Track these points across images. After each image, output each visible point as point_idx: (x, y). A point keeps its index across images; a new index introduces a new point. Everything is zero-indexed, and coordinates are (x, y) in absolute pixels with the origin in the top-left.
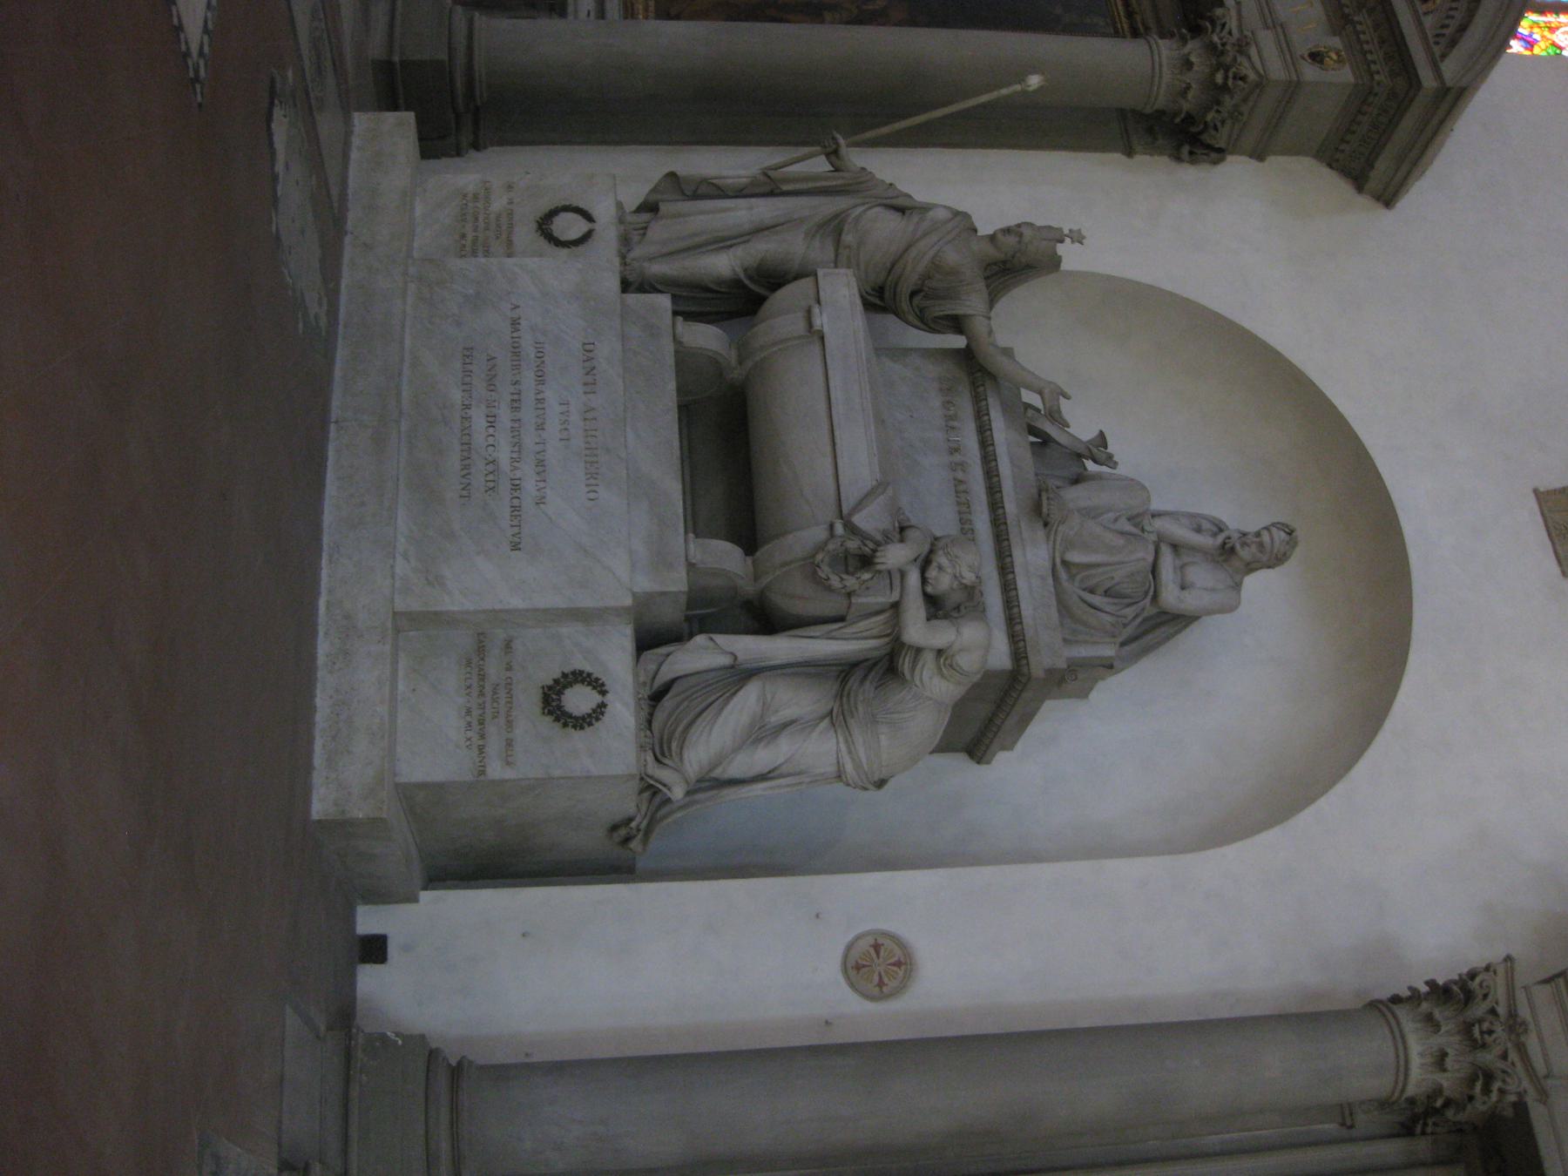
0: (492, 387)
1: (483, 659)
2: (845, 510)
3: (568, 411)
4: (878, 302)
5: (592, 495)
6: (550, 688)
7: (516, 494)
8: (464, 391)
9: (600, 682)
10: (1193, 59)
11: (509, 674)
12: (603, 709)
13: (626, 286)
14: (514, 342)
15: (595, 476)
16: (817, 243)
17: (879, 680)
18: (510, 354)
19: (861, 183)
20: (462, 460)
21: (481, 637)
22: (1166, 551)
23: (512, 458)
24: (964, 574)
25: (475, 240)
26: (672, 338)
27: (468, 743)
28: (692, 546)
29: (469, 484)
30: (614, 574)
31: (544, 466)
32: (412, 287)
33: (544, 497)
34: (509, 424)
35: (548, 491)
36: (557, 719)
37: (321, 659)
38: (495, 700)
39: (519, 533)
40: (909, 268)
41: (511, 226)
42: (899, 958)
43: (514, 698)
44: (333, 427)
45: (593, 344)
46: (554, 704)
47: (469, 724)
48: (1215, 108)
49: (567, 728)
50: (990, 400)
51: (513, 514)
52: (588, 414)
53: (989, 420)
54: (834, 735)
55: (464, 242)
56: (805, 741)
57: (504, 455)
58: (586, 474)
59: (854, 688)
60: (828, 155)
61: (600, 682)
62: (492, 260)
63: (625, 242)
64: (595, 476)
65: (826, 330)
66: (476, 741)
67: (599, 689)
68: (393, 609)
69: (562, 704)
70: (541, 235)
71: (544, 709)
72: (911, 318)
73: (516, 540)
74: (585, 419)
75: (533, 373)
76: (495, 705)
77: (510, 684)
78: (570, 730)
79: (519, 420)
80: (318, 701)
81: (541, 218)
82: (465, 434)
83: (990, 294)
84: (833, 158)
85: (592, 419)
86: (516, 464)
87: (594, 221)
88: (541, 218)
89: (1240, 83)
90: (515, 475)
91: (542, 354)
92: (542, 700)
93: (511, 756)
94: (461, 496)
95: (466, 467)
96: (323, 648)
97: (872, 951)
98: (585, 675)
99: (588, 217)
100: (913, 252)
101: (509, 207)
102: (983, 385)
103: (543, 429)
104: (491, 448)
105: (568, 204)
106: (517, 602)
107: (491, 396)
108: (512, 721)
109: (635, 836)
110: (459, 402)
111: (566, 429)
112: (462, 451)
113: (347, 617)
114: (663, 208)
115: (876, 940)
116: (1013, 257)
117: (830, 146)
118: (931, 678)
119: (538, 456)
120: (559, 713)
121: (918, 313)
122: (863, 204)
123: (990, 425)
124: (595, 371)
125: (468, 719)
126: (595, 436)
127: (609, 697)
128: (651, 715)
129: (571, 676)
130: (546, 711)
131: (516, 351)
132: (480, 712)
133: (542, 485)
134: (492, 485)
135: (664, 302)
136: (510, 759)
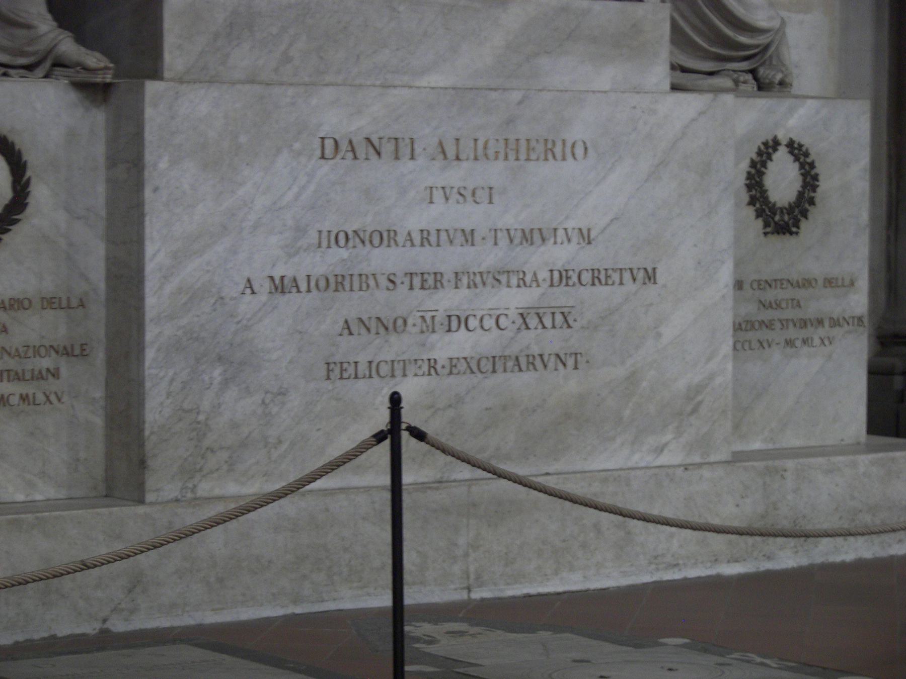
0: (400, 322)
3: (443, 188)
5: (579, 151)
6: (766, 225)
7: (575, 278)
8: (405, 375)
12: (796, 146)
14: (317, 286)
18: (342, 295)
20: (520, 370)
23: (519, 286)
27: (827, 342)
29: (558, 356)
30: (693, 120)
31: (532, 230)
33: (580, 230)
34: (464, 292)
35: (570, 224)
36: (805, 214)
38: (779, 306)
43: (779, 277)
44: (478, 594)
47: (805, 341)
49: (817, 200)
51: (603, 281)
55: (15, 400)
58: (546, 159)
61: (762, 147)
62: (149, 336)
66: (822, 332)
67: (770, 150)
68: (726, 462)
69: (787, 205)
71: (791, 233)
73: (641, 275)
74: (458, 158)
76: (784, 305)
77: (759, 281)
78: (818, 195)
79: (456, 273)
82: (479, 369)
86: (528, 279)
90: (544, 280)
91: (342, 237)
93: (843, 279)
94: (576, 368)
95: (531, 364)
104: (503, 321)
106: (726, 274)
107: (414, 325)
110: (424, 380)
111: (474, 194)
112: (505, 371)
119: (517, 241)
120: (797, 212)
125: (798, 343)
129: (754, 192)
130: (794, 229)
132: (791, 325)
133: (561, 233)
136: (847, 282)
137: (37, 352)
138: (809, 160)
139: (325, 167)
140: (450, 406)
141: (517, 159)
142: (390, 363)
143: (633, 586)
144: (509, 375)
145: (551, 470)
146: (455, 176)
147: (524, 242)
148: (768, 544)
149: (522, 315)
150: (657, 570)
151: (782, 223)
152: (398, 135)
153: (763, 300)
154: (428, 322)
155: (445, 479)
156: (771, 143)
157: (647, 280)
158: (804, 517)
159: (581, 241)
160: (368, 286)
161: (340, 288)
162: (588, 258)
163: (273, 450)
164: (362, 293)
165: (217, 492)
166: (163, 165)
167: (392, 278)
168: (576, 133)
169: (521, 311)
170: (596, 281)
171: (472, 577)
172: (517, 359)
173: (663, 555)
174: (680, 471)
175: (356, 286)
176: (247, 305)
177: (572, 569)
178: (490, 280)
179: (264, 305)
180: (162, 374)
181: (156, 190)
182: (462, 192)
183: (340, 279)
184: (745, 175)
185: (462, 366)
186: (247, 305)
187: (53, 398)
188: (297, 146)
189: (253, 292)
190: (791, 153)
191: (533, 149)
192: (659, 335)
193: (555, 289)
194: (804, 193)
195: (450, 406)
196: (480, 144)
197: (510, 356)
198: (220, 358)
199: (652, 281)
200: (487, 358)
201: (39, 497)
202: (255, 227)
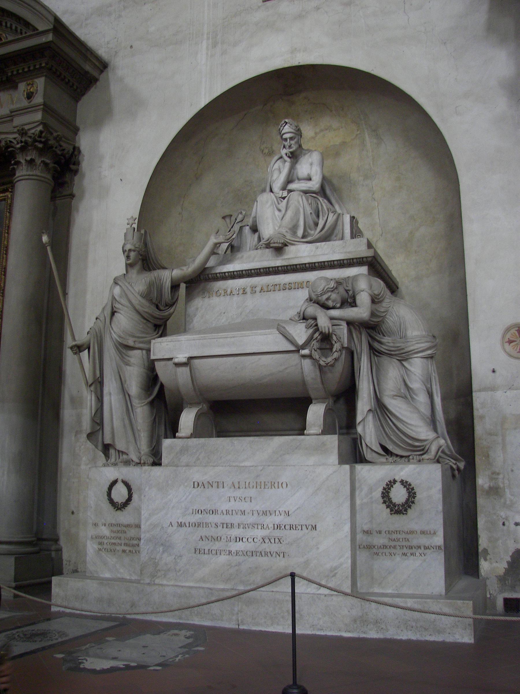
0: (219, 538)
1: (374, 547)
2: (293, 348)
3: (234, 497)
4: (162, 328)
5: (284, 485)
6: (391, 510)
7: (283, 527)
8: (220, 554)
9: (388, 483)
10: (29, 158)
11: (383, 532)
12: (404, 482)
13: (157, 463)
15: (273, 484)
16: (132, 360)
17: (380, 334)
18: (200, 528)
19: (97, 334)
20: (262, 556)
21: (362, 547)
22: (291, 186)
23: (261, 529)
24: (332, 287)
25: (126, 545)
26: (189, 439)
27: (423, 555)
28: (312, 432)
31: (266, 511)
32: (157, 581)
33: (285, 511)
34: (241, 530)
36: (410, 507)
37: (380, 636)
39: (306, 526)
40: (146, 310)
41: (119, 525)
42: (516, 330)
43: (398, 529)
44: (241, 627)
45: (194, 482)
46: (401, 508)
48: (54, 149)
50: (218, 271)
51: (294, 528)
52: (236, 486)
53: (228, 272)
54: (413, 359)
55: (127, 551)
56: (415, 375)
57: (259, 533)
59: (386, 348)
60: (80, 351)
61: (388, 483)
62: (142, 537)
63: (128, 463)
64: (273, 484)
65: (187, 355)
67: (392, 484)
69: (401, 504)
70: (125, 509)
71: (403, 514)
72: (172, 310)
73: (310, 527)
75: (211, 516)
76: (401, 540)
80: (404, 638)
81: (114, 508)
83: (159, 269)
84: (82, 349)
85: (239, 484)
86: (265, 527)
87: (117, 479)
88: (114, 508)
89: (43, 135)
90: (271, 527)
92: (399, 514)
95: (266, 554)
96: (373, 634)
97: (512, 344)
98: (384, 491)
99: (115, 482)
100: (138, 307)
101: (107, 525)
102: (208, 275)
103: (244, 511)
105: (106, 494)
107: (224, 539)
108: (410, 531)
109: (457, 466)
110: (227, 557)
111: (245, 499)
113: (355, 621)
114: (107, 441)
115: (506, 342)
116: (141, 255)
117: (76, 350)
118: (383, 307)
119: (261, 514)
120: (406, 506)
121: (168, 307)
122: (111, 333)
123: (231, 272)
124: (211, 482)
126: (249, 483)
127: (397, 478)
128: (397, 456)
129: (385, 499)
130: (405, 512)
131: (198, 525)
132: (405, 548)
133: (277, 512)
134: (277, 540)
135: (167, 443)
136: (432, 532)
137: (133, 539)
138: (411, 487)
139: (195, 490)
140: (236, 565)
141: (261, 488)
142: (216, 551)
143: (303, 634)
144: (257, 557)
145: (274, 590)
146: (238, 493)
147: (263, 514)
148: (364, 628)
149: (263, 538)
150: (314, 630)
151: (399, 510)
152: (219, 481)
153: (391, 538)
154: (229, 538)
155: (235, 588)
156: (392, 481)
157: (312, 529)
158: (381, 619)
159: (285, 515)
160: (208, 527)
161: (199, 526)
162: (288, 521)
163: (178, 573)
164: (206, 528)
165: (161, 582)
166: (147, 489)
167: (216, 524)
168: (283, 479)
169: (263, 537)
170: (292, 528)
171: (240, 621)
172: (261, 552)
173: (316, 625)
174: (323, 597)
175: (204, 526)
176: (170, 530)
177: (278, 624)
178: (251, 526)
179: (176, 530)
180: (145, 547)
181: (145, 496)
182: (240, 498)
183: (199, 524)
184: (381, 493)
185: (241, 553)
186: (170, 530)
187: (137, 552)
188: (186, 484)
189: (172, 526)
190: (402, 484)
191: (267, 485)
192: (318, 548)
193: (275, 530)
194: (409, 499)
195: (236, 565)
196: (247, 484)
197: (258, 552)
198: (162, 544)
199: (315, 529)
200: (250, 551)
201: (133, 578)
202: (173, 507)
